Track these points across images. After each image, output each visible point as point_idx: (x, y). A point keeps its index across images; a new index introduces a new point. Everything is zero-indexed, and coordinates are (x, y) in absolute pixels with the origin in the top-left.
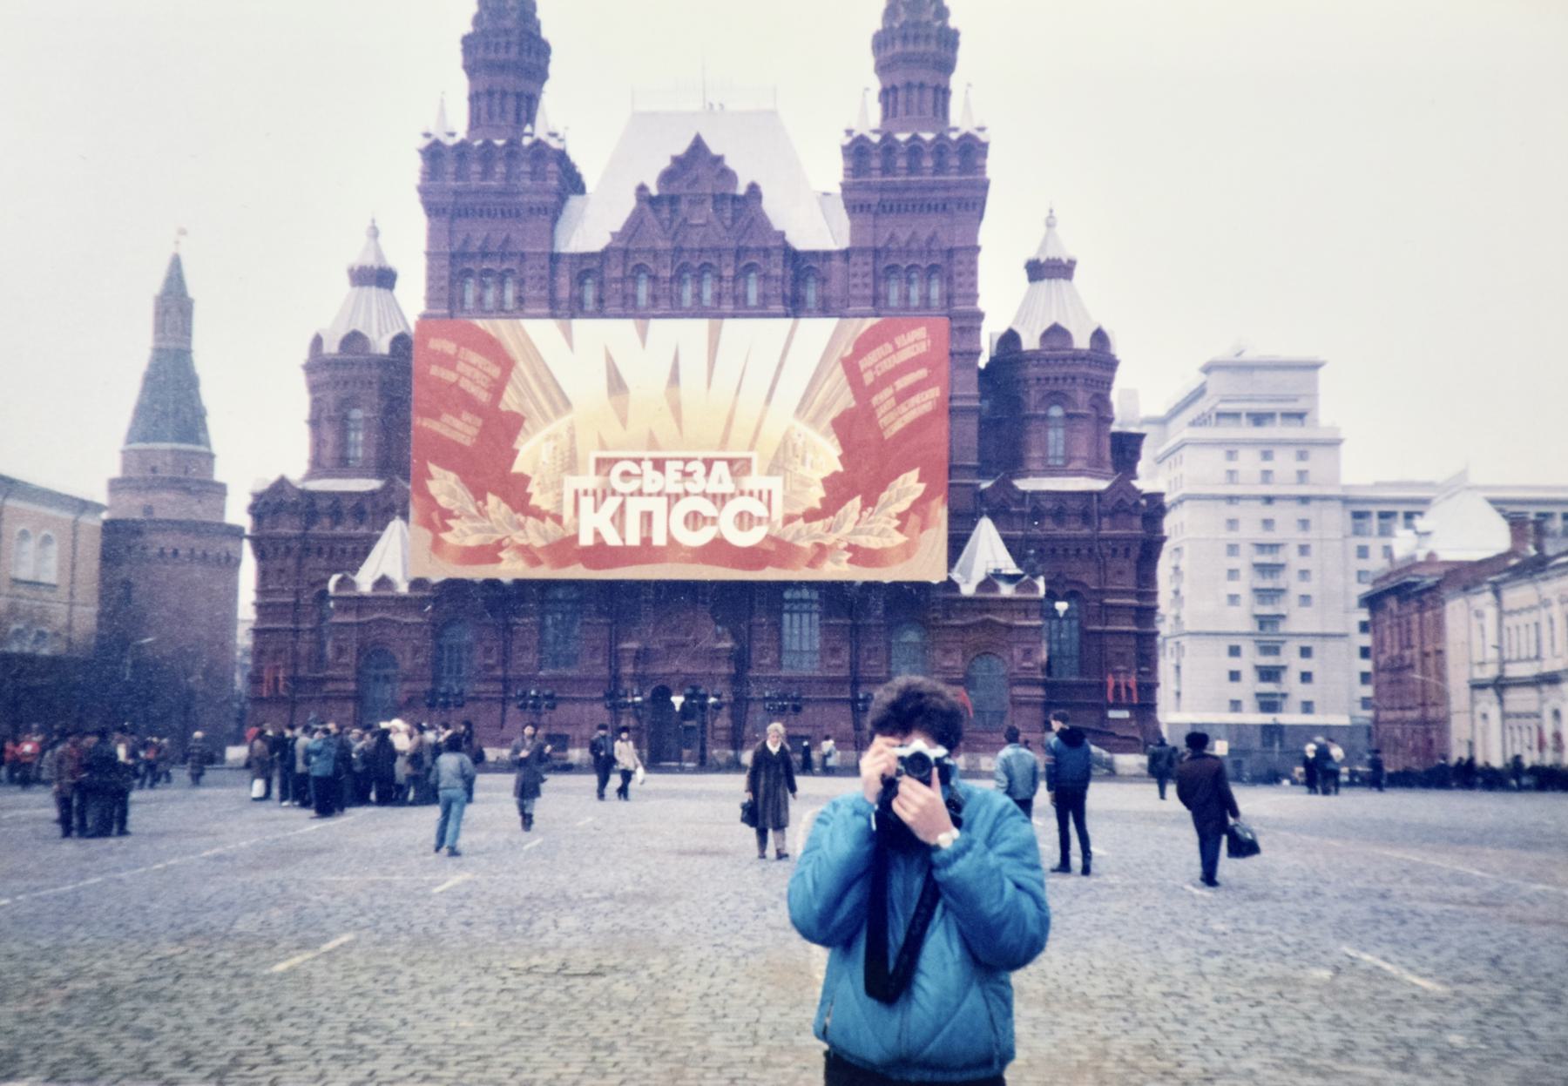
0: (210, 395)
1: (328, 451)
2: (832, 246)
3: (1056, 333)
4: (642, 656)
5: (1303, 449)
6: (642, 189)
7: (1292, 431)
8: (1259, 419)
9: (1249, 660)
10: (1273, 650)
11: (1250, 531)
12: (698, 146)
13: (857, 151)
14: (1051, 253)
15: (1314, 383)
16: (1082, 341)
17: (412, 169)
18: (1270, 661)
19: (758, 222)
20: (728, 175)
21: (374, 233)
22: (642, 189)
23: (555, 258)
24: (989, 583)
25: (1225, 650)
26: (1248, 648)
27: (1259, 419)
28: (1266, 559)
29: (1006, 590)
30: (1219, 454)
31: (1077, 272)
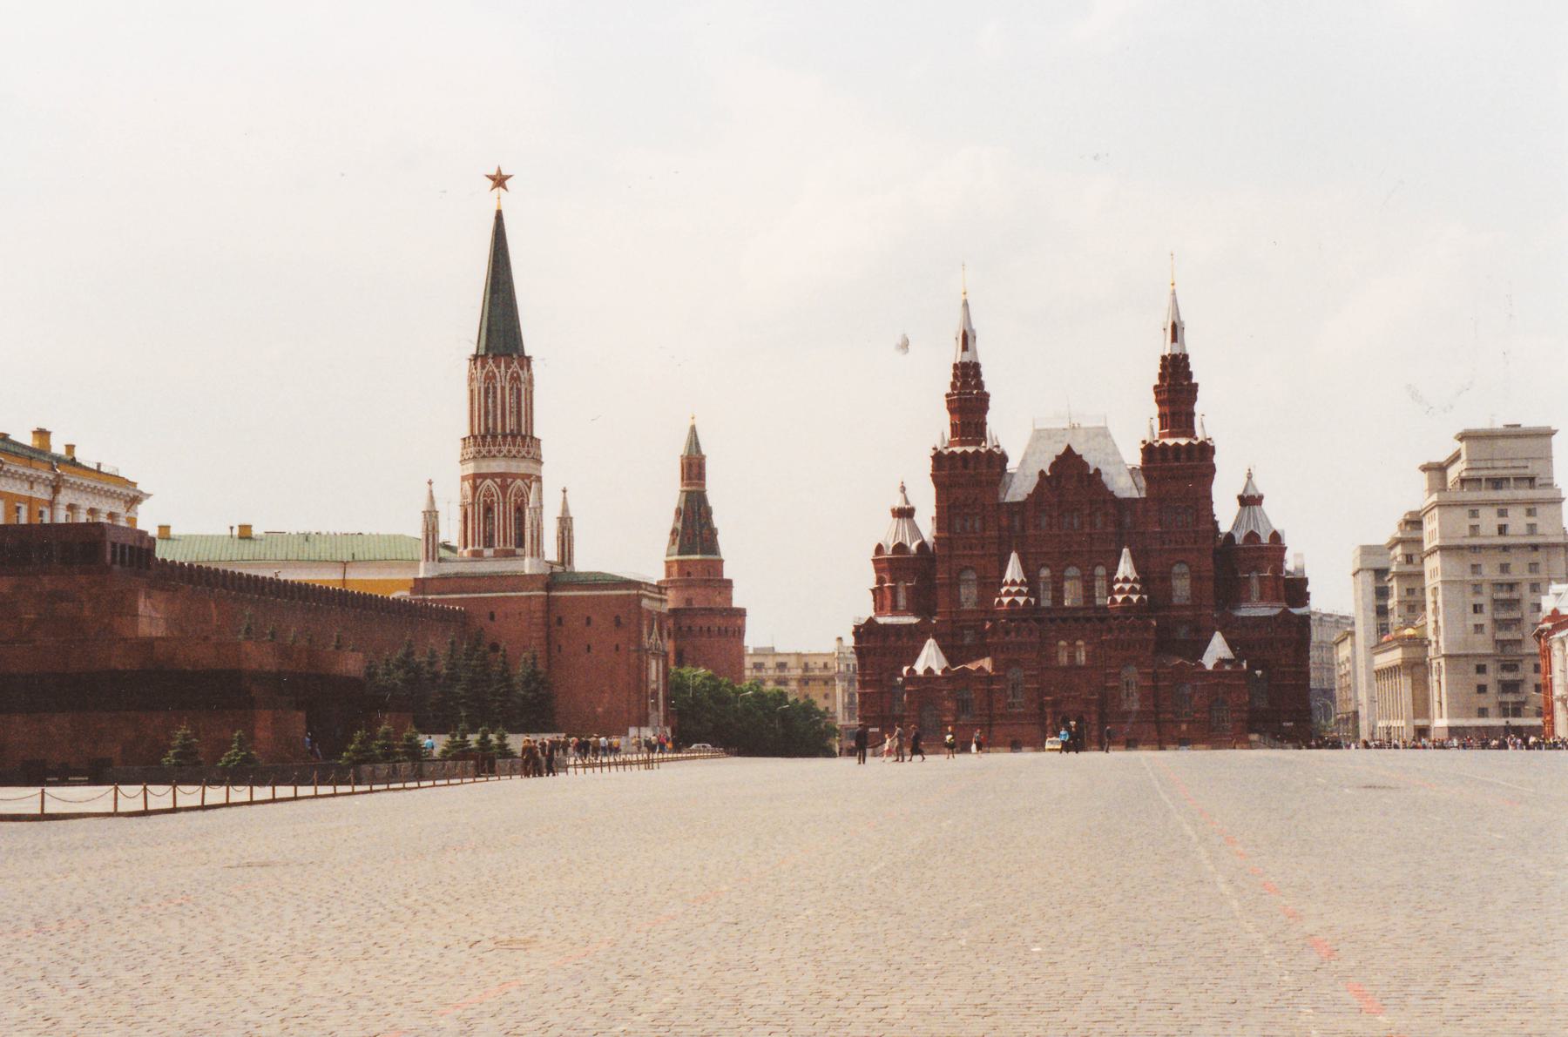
0: (717, 520)
1: (888, 602)
2: (1135, 494)
3: (1252, 537)
4: (1055, 703)
5: (1531, 508)
6: (1042, 473)
7: (1524, 493)
8: (1497, 483)
9: (1491, 678)
10: (1511, 667)
11: (1490, 572)
12: (1069, 449)
13: (1149, 450)
14: (1251, 492)
15: (1549, 447)
16: (1265, 539)
17: (927, 466)
18: (1508, 676)
19: (1103, 486)
20: (1085, 465)
21: (903, 489)
22: (1042, 473)
23: (1000, 505)
24: (1222, 662)
25: (1472, 669)
26: (1491, 667)
27: (1497, 483)
28: (1503, 595)
29: (1227, 668)
30: (1463, 513)
31: (1264, 501)
